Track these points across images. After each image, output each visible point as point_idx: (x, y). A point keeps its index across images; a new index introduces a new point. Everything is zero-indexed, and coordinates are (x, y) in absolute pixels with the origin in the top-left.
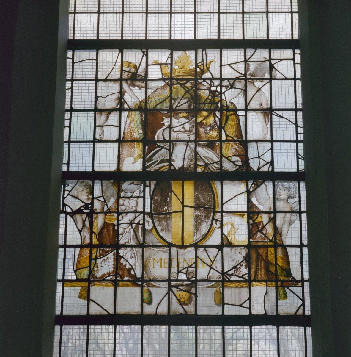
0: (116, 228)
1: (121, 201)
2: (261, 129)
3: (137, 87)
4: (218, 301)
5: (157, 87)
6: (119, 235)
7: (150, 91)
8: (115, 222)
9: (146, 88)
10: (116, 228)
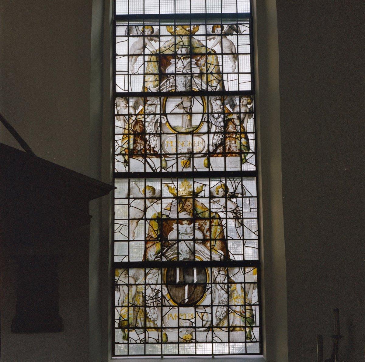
0: (144, 123)
1: (146, 107)
2: (231, 66)
3: (154, 41)
4: (206, 165)
5: (166, 41)
6: (146, 127)
7: (162, 44)
8: (143, 120)
9: (160, 41)
10: (144, 123)
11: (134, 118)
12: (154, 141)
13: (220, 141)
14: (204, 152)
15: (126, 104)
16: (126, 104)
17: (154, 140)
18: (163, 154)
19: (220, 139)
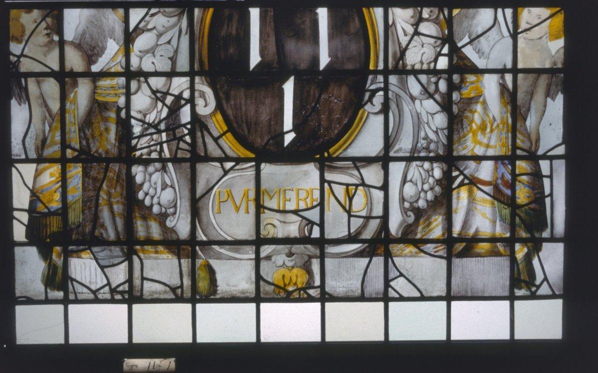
11: (82, 93)
12: (162, 189)
13: (432, 189)
14: (368, 234)
15: (48, 35)
16: (48, 35)
17: (164, 187)
18: (203, 244)
19: (431, 180)
